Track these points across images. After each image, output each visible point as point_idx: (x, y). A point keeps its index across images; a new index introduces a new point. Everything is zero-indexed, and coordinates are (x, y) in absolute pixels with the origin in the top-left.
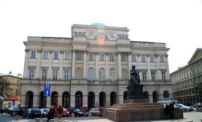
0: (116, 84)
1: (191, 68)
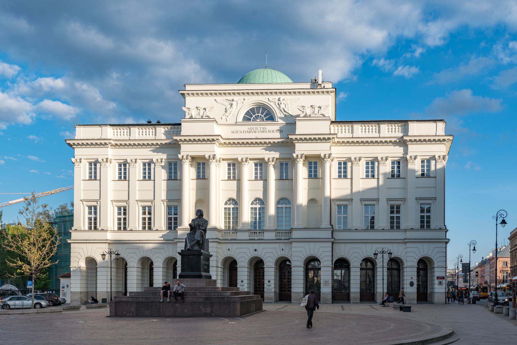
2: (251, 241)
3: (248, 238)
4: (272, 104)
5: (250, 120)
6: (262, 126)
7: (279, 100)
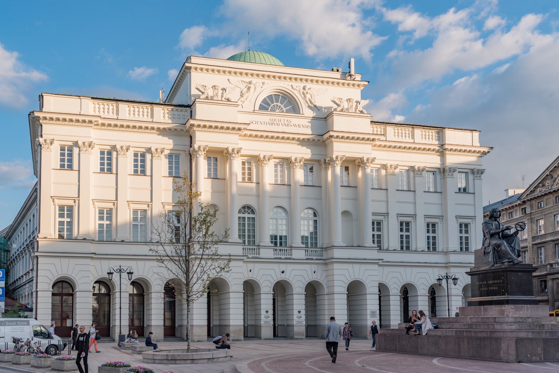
0: (321, 259)
1: (528, 211)
2: (277, 261)
3: (274, 257)
4: (295, 92)
5: (267, 109)
6: (286, 119)
7: (304, 88)
